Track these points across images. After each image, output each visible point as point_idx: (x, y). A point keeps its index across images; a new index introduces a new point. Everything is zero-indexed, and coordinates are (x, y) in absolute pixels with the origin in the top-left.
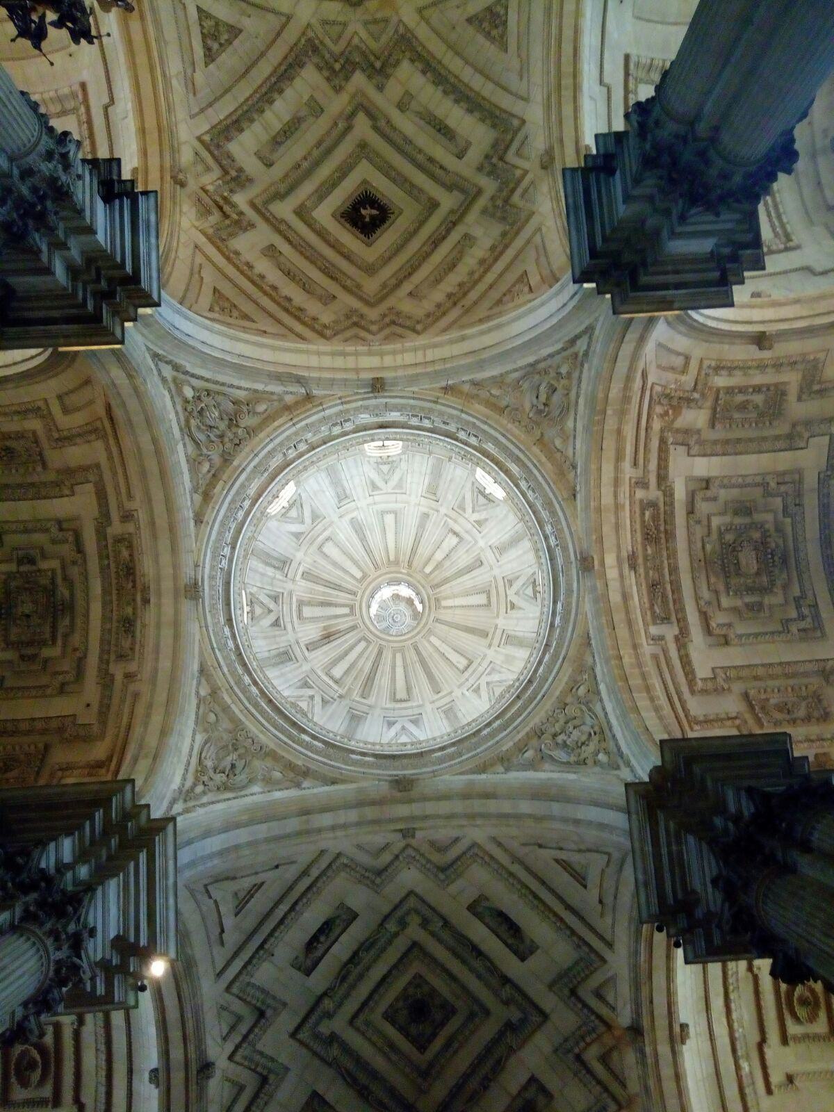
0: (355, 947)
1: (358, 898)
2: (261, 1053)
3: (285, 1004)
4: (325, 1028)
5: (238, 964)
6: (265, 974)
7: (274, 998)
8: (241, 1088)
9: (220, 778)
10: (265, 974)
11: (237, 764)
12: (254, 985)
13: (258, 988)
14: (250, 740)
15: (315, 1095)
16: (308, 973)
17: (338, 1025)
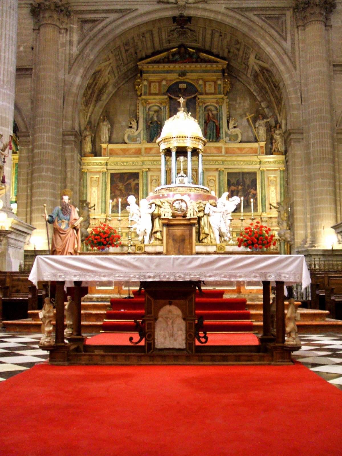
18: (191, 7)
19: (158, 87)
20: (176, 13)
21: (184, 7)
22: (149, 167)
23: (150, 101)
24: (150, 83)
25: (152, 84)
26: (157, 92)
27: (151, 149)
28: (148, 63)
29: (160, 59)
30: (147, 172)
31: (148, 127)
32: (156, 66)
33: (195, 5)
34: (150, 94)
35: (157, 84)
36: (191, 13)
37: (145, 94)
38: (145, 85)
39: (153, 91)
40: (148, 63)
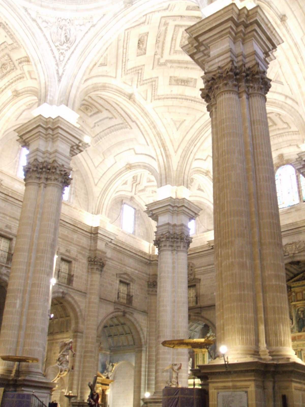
0: (155, 39)
1: (143, 29)
2: (146, 80)
3: (144, 65)
4: (162, 61)
5: (119, 71)
6: (130, 65)
7: (139, 67)
8: (147, 90)
9: (65, 46)
10: (130, 65)
11: (67, 35)
12: (129, 70)
13: (131, 69)
14: (64, 21)
15: (171, 77)
16: (145, 53)
17: (166, 56)
18: (297, 256)
19: (301, 296)
20: (290, 260)
21: (293, 257)
22: (301, 348)
23: (298, 305)
24: (296, 294)
25: (298, 294)
26: (301, 298)
27: (301, 336)
28: (293, 282)
29: (299, 278)
30: (301, 351)
31: (298, 322)
32: (297, 283)
33: (299, 254)
34: (298, 301)
35: (301, 294)
36: (298, 259)
37: (294, 301)
38: (294, 296)
39: (299, 298)
40: (293, 282)
